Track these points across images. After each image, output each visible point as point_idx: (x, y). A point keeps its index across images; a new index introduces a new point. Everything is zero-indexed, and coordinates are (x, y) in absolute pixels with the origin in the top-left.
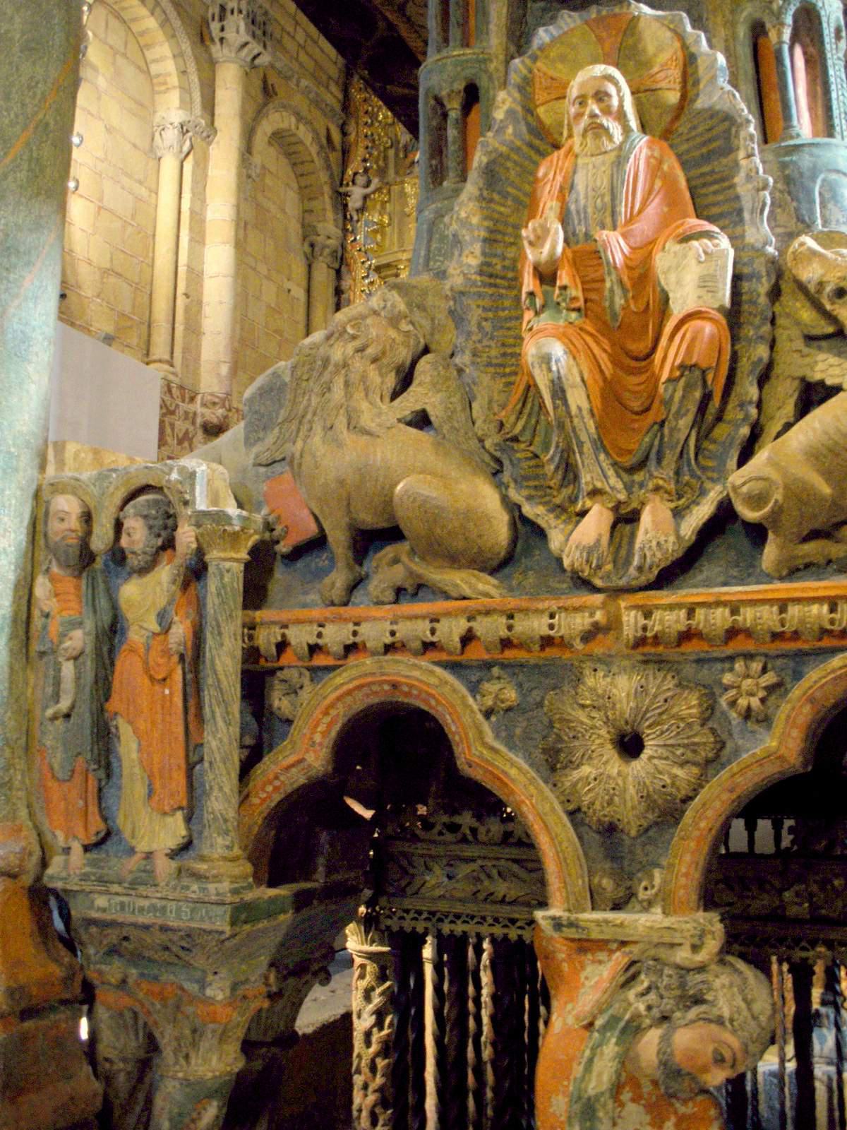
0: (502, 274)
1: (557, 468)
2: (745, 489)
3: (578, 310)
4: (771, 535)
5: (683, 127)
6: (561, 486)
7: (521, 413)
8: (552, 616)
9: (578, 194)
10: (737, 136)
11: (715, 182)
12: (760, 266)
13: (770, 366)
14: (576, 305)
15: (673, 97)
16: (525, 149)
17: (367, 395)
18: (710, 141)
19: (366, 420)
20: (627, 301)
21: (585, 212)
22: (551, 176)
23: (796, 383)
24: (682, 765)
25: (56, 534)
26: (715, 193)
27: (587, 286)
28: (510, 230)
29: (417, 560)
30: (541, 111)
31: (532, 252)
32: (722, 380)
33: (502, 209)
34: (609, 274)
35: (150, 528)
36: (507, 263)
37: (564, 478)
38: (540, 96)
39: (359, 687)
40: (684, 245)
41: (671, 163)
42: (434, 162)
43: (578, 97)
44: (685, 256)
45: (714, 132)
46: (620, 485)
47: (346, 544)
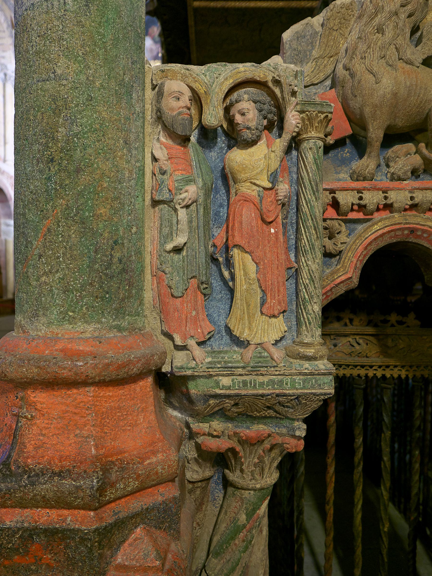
25: (172, 109)
35: (260, 111)
39: (389, 232)
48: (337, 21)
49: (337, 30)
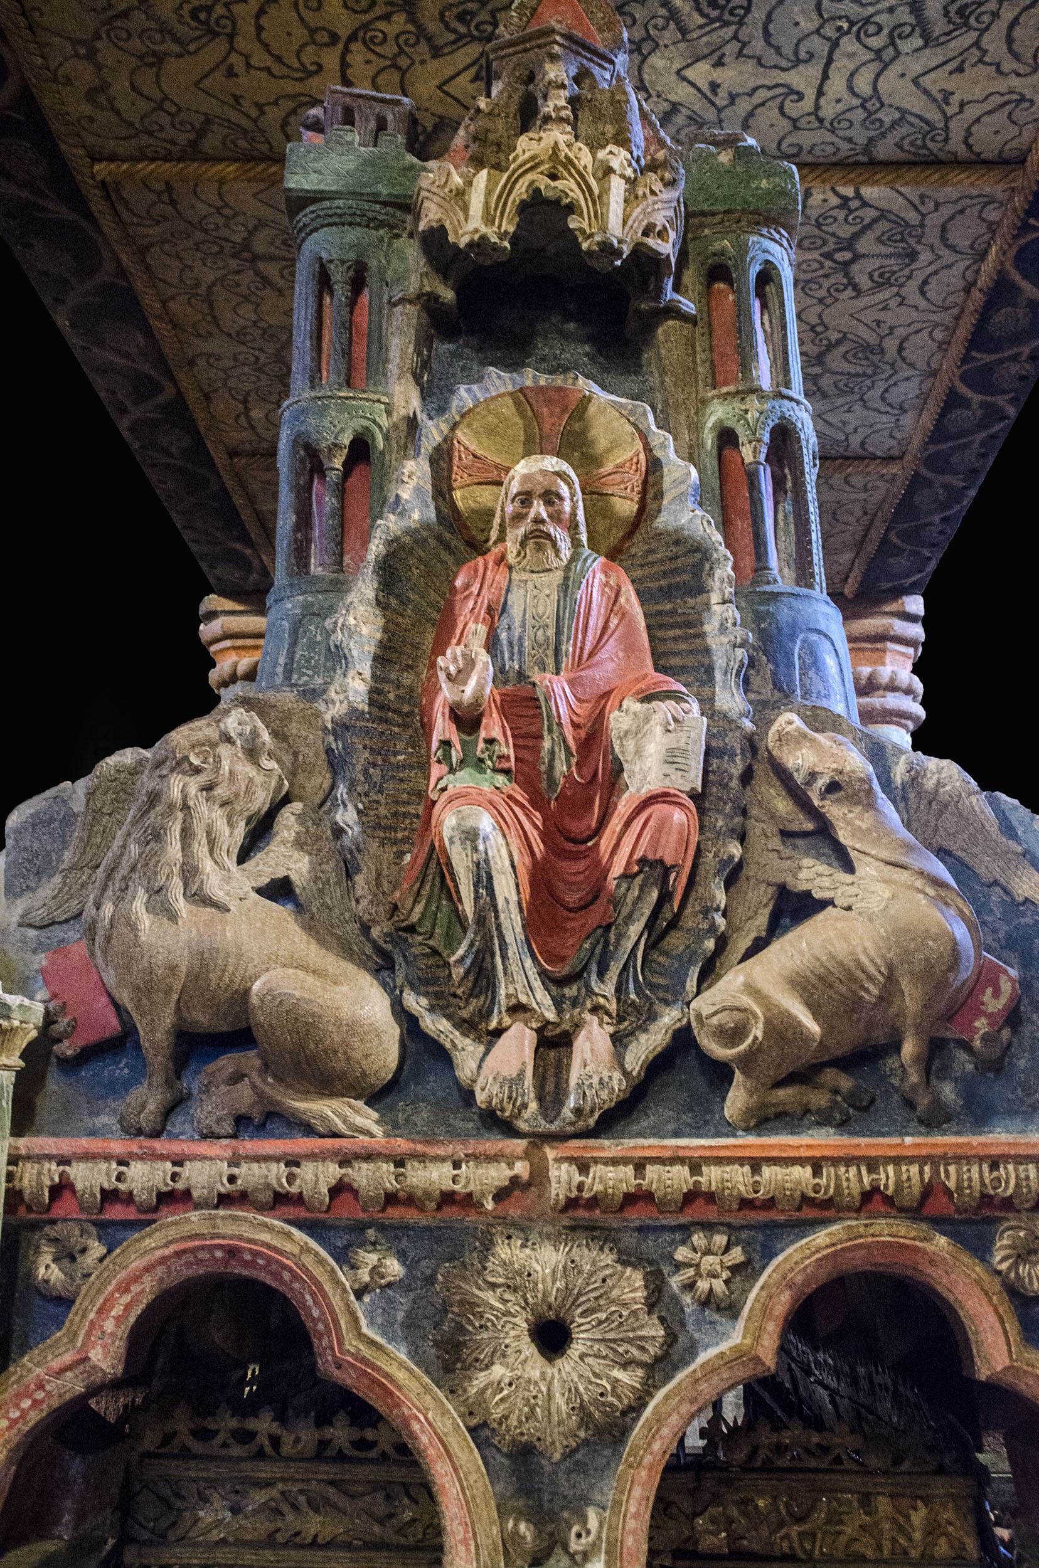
0: (395, 706)
1: (467, 973)
2: (715, 1021)
3: (506, 772)
4: (738, 1077)
5: (637, 548)
6: (471, 995)
7: (418, 893)
8: (457, 1165)
9: (512, 619)
10: (711, 574)
11: (679, 626)
12: (734, 741)
13: (739, 866)
14: (505, 765)
15: (626, 507)
16: (432, 542)
17: (211, 852)
18: (674, 571)
19: (213, 881)
20: (569, 767)
21: (521, 645)
22: (475, 589)
23: (771, 890)
24: (625, 1366)
26: (675, 639)
27: (521, 742)
28: (408, 649)
29: (270, 1080)
30: (457, 495)
31: (451, 690)
32: (684, 880)
33: (400, 620)
34: (550, 731)
36: (402, 691)
37: (474, 986)
38: (459, 477)
39: (178, 1254)
40: (646, 706)
41: (630, 599)
42: (299, 535)
43: (519, 494)
44: (647, 720)
45: (679, 563)
46: (548, 1001)
47: (168, 1052)
48: (111, 796)
49: (110, 814)
